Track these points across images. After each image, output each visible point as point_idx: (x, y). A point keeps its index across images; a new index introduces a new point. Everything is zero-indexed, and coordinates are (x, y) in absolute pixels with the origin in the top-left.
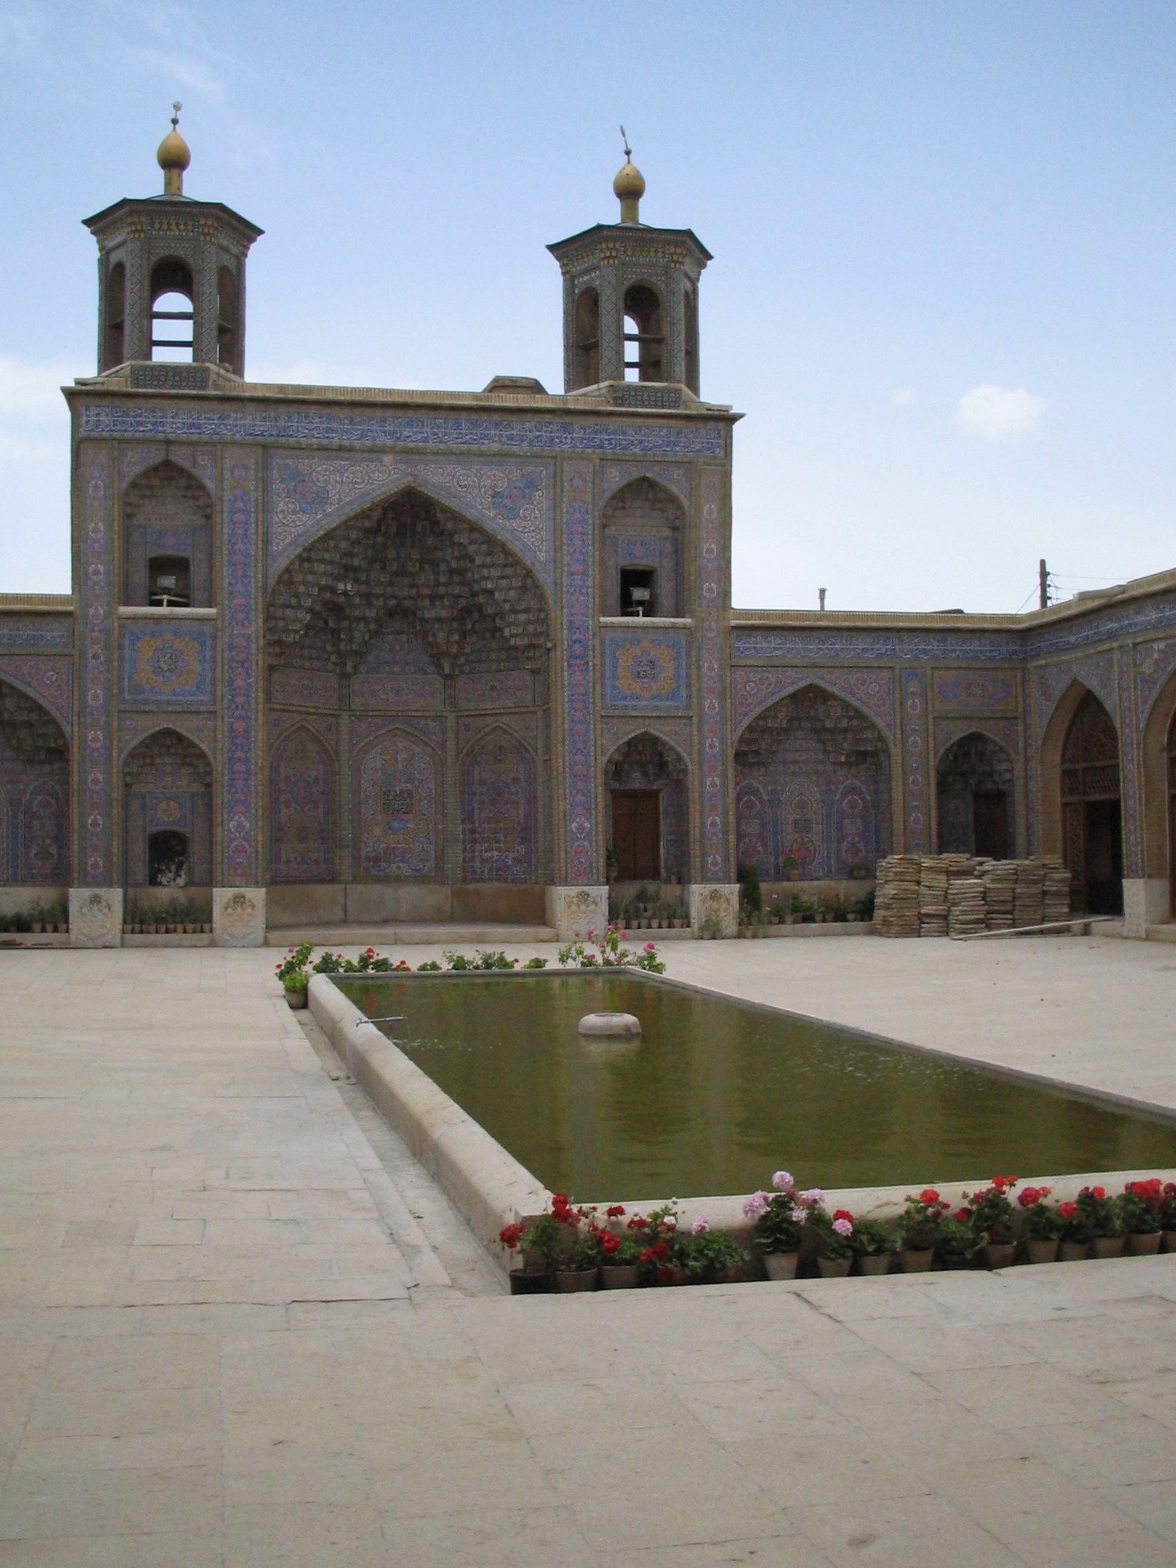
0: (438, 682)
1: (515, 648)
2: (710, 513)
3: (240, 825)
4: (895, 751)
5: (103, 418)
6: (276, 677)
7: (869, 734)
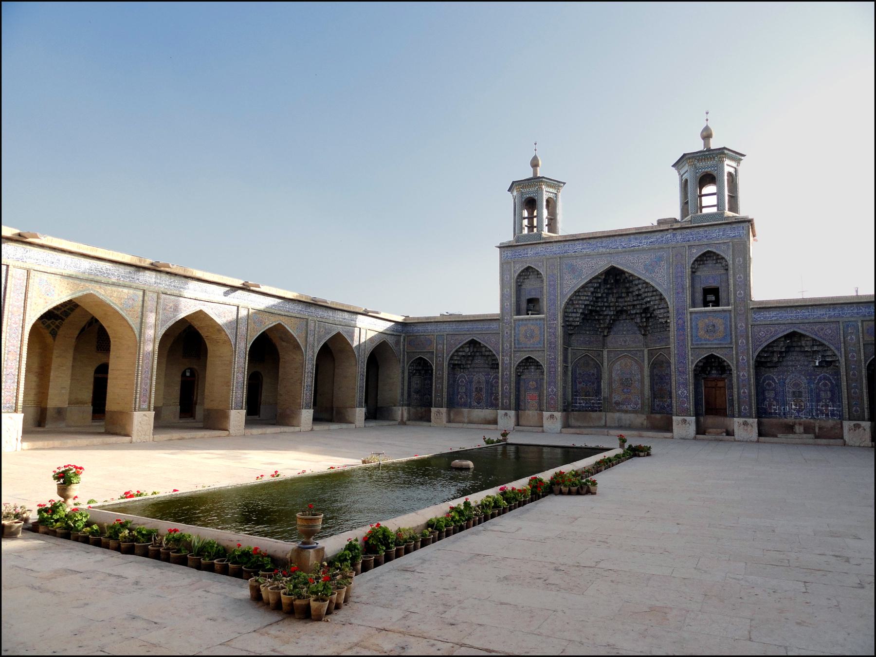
0: (641, 337)
1: (661, 323)
2: (739, 261)
3: (552, 391)
4: (842, 361)
5: (509, 253)
6: (573, 337)
7: (829, 353)
